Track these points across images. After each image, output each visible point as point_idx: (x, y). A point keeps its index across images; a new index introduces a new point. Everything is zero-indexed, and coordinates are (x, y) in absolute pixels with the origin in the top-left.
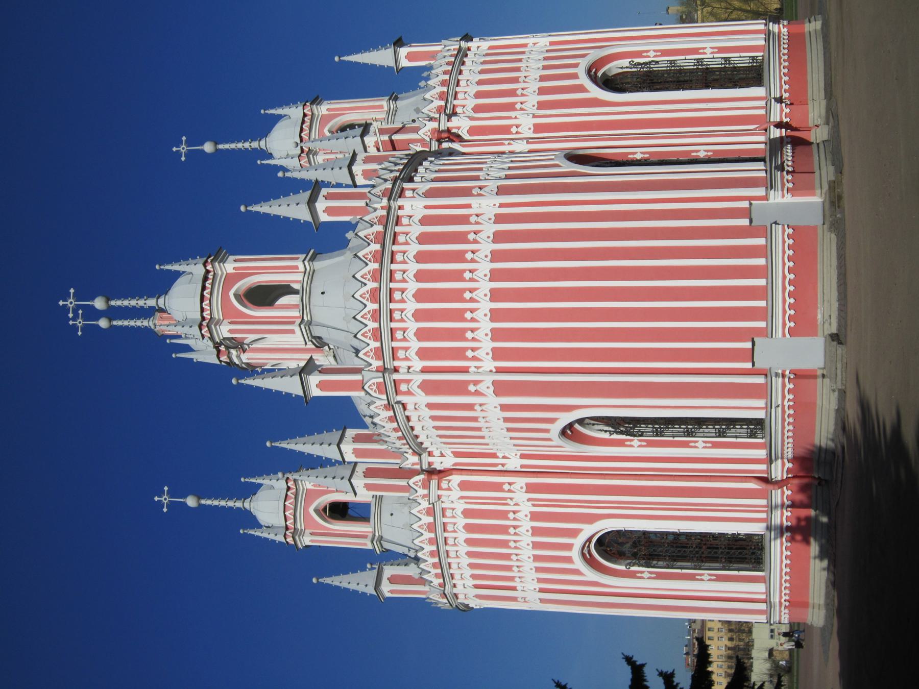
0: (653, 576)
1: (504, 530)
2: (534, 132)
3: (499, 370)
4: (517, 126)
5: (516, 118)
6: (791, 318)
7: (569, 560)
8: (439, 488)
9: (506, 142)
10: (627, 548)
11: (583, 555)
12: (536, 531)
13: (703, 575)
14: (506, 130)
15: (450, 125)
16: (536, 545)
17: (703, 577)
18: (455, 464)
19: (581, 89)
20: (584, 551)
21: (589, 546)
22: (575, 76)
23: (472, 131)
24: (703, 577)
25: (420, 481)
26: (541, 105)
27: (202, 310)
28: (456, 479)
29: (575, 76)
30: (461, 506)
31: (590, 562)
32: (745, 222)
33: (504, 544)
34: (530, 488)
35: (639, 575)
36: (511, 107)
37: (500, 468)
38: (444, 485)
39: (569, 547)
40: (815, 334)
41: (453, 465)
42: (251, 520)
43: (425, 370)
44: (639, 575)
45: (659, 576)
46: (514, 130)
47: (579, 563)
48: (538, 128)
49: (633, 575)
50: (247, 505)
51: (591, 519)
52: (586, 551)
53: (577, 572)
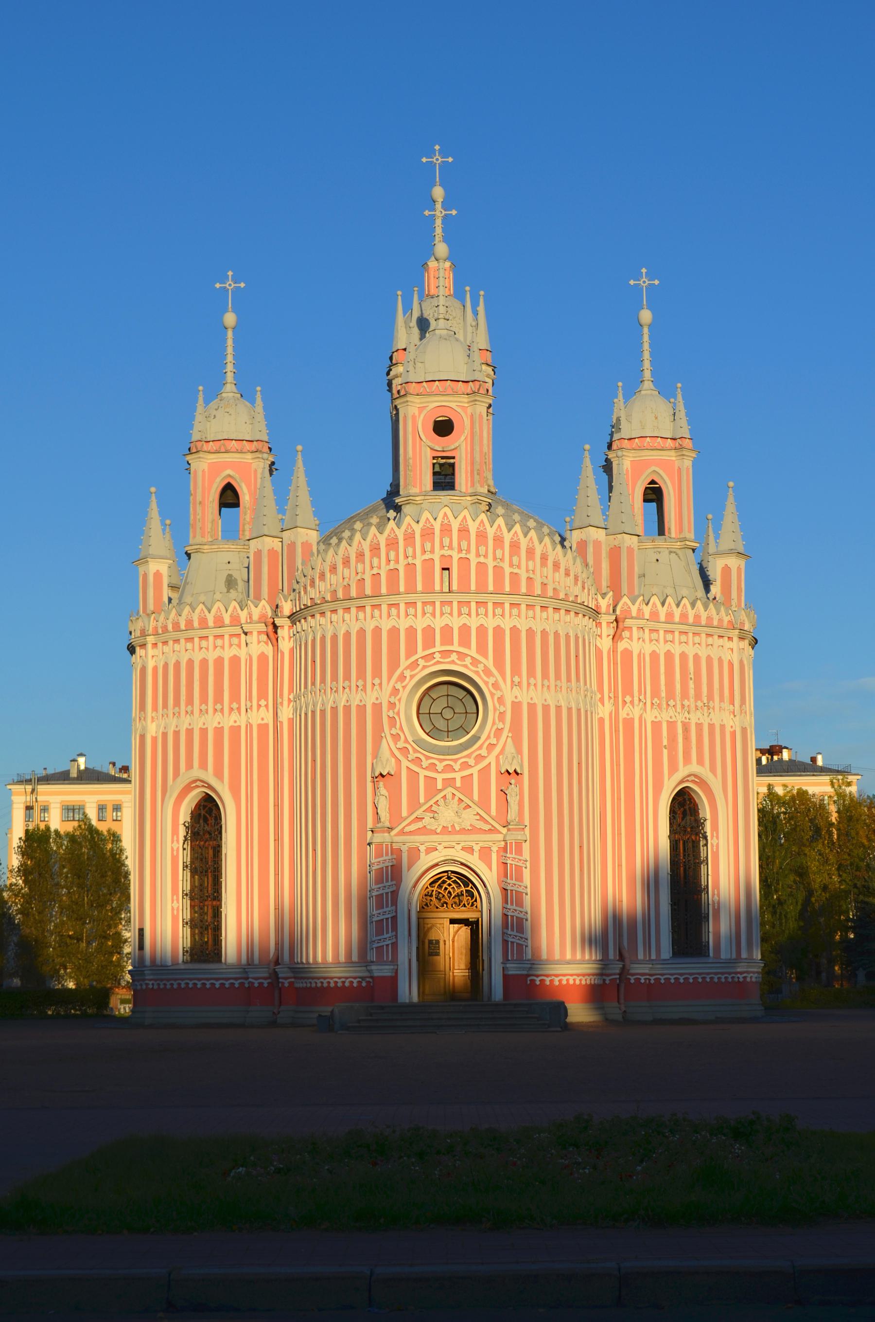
0: (175, 853)
1: (219, 699)
2: (624, 719)
4: (632, 702)
5: (640, 700)
7: (189, 766)
8: (259, 633)
9: (612, 695)
11: (195, 781)
12: (219, 731)
13: (178, 902)
15: (635, 630)
16: (204, 732)
17: (175, 902)
18: (282, 653)
19: (673, 769)
20: (198, 782)
21: (203, 786)
22: (687, 760)
23: (628, 654)
24: (175, 902)
25: (266, 612)
26: (656, 725)
28: (269, 650)
29: (687, 760)
30: (243, 653)
31: (187, 789)
33: (204, 700)
34: (263, 728)
35: (175, 838)
36: (655, 693)
37: (279, 700)
38: (264, 637)
39: (203, 765)
41: (281, 651)
44: (175, 838)
45: (175, 859)
46: (628, 699)
48: (629, 723)
49: (175, 832)
52: (199, 783)
53: (176, 773)
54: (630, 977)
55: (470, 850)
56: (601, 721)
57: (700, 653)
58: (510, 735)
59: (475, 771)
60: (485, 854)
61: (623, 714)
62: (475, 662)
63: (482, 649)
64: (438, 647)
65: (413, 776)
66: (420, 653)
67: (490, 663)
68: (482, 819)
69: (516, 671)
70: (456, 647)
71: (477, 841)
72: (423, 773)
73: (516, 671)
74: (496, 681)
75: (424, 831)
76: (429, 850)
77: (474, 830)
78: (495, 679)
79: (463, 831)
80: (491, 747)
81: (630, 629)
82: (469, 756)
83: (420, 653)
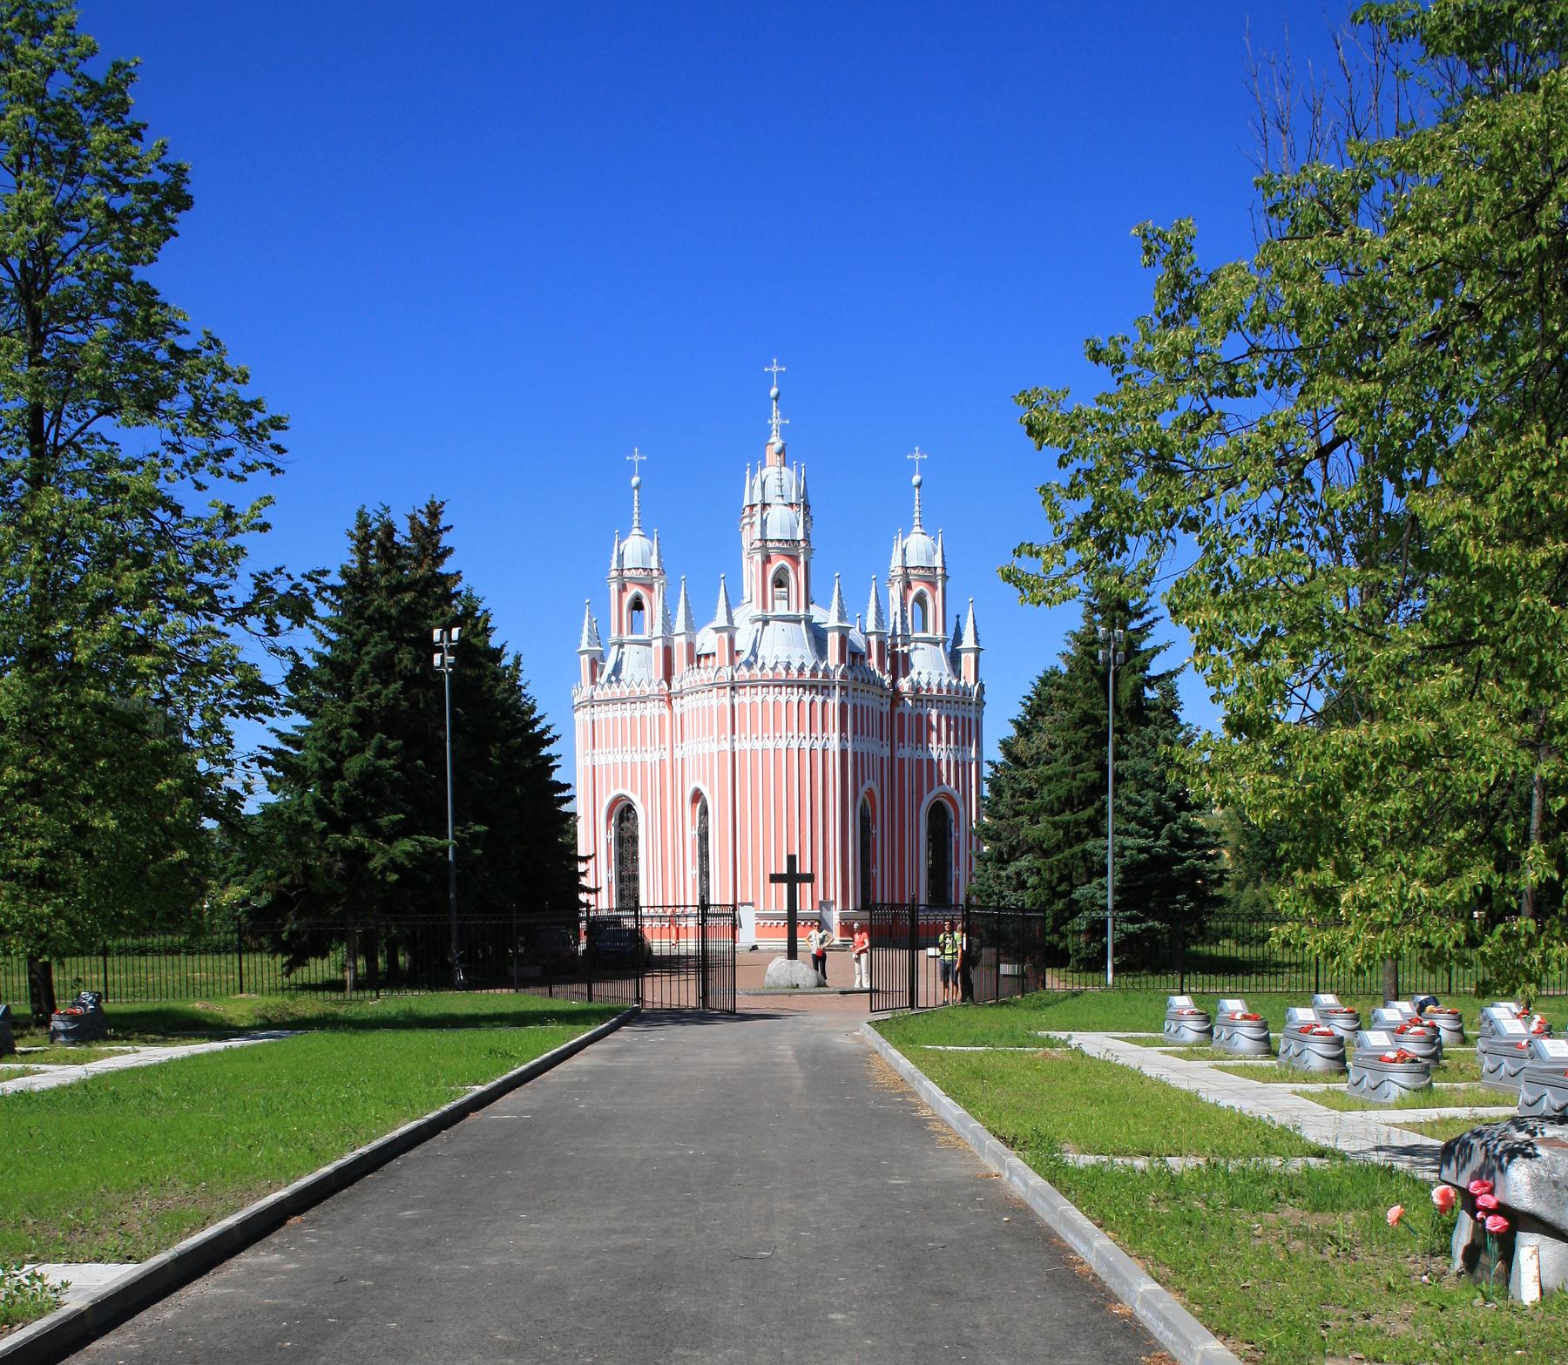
3: (734, 754)
10: (625, 824)
14: (901, 739)
19: (930, 788)
27: (772, 541)
28: (666, 712)
30: (647, 713)
32: (821, 898)
39: (624, 786)
40: (757, 936)
42: (625, 535)
43: (733, 707)
45: (608, 845)
47: (614, 794)
48: (902, 761)
50: (636, 531)
51: (644, 800)
53: (608, 793)
56: (882, 759)
61: (898, 755)
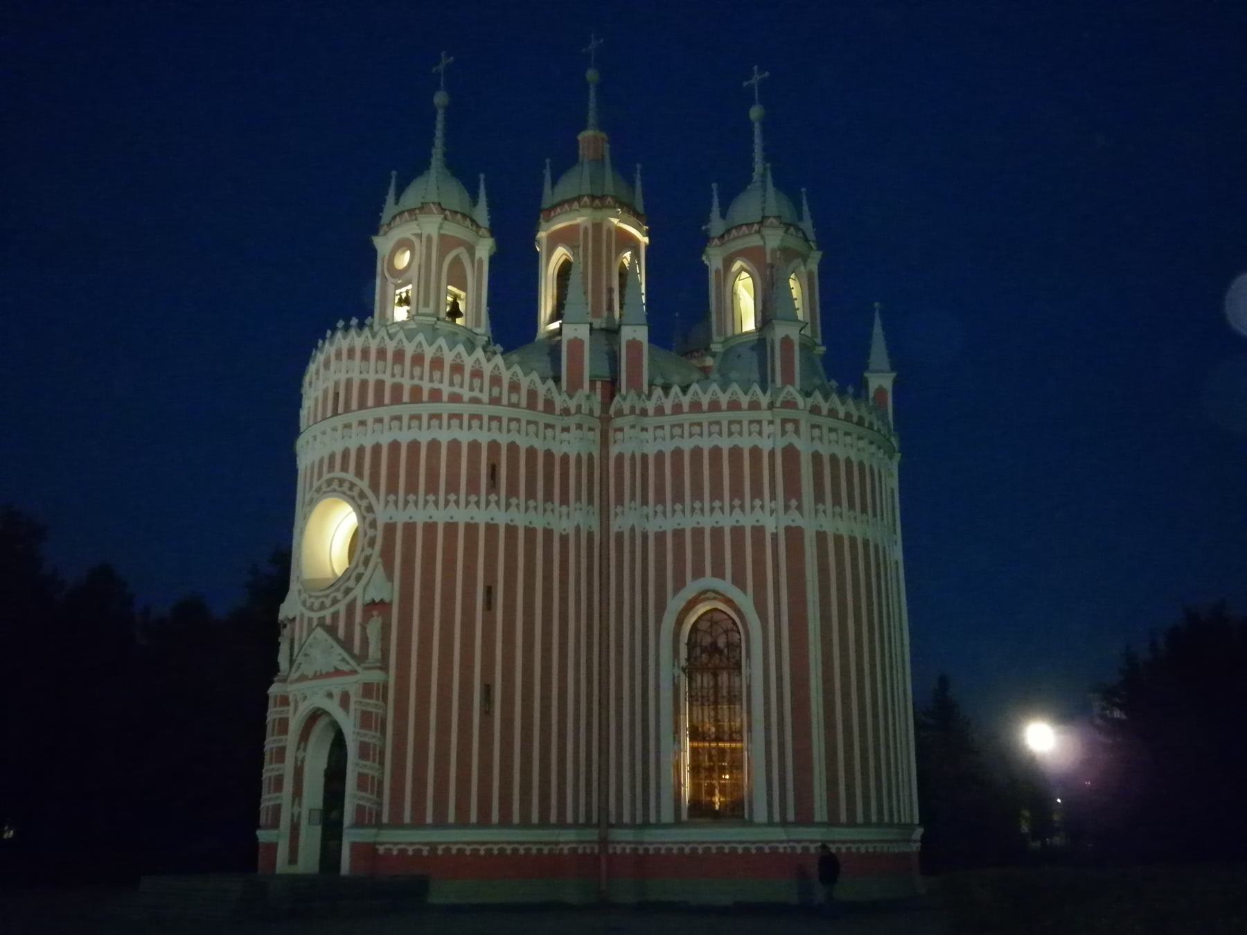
6: (528, 850)
14: (620, 501)
19: (680, 584)
54: (615, 845)
55: (330, 695)
57: (822, 451)
58: (380, 560)
59: (341, 607)
60: (345, 701)
61: (614, 527)
62: (352, 486)
63: (359, 474)
64: (326, 476)
65: (302, 615)
66: (316, 484)
67: (364, 484)
68: (343, 660)
69: (392, 488)
70: (337, 473)
71: (337, 685)
72: (308, 614)
73: (392, 488)
74: (370, 503)
75: (303, 678)
76: (305, 698)
77: (338, 672)
78: (367, 501)
79: (328, 675)
80: (359, 577)
81: (621, 430)
82: (338, 590)
83: (316, 484)
